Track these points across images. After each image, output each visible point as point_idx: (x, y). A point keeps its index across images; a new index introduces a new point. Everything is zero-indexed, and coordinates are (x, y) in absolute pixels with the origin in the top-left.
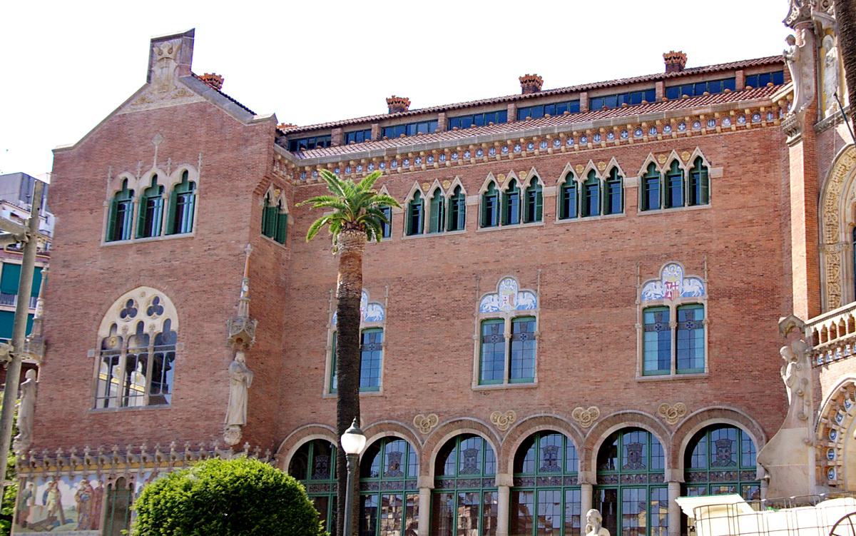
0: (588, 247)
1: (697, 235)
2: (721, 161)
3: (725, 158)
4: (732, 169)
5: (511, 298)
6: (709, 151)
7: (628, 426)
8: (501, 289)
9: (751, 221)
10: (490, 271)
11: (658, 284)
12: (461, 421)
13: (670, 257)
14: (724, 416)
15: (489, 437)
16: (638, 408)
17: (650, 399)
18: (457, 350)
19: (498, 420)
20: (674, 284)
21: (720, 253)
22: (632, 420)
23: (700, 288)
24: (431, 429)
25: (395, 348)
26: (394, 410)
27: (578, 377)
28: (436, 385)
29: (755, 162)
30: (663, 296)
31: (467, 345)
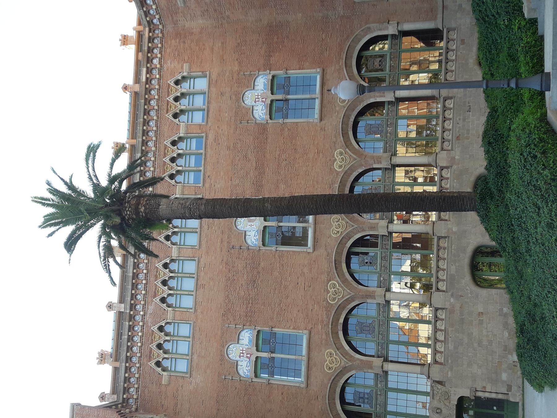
2: (180, 65)
3: (178, 63)
4: (186, 58)
6: (172, 74)
7: (351, 129)
8: (242, 229)
10: (228, 238)
11: (255, 108)
13: (239, 97)
15: (350, 238)
16: (339, 120)
17: (334, 112)
18: (283, 265)
19: (338, 230)
20: (257, 97)
22: (347, 125)
23: (262, 77)
24: (339, 288)
25: (275, 319)
27: (312, 167)
30: (264, 104)
31: (279, 256)
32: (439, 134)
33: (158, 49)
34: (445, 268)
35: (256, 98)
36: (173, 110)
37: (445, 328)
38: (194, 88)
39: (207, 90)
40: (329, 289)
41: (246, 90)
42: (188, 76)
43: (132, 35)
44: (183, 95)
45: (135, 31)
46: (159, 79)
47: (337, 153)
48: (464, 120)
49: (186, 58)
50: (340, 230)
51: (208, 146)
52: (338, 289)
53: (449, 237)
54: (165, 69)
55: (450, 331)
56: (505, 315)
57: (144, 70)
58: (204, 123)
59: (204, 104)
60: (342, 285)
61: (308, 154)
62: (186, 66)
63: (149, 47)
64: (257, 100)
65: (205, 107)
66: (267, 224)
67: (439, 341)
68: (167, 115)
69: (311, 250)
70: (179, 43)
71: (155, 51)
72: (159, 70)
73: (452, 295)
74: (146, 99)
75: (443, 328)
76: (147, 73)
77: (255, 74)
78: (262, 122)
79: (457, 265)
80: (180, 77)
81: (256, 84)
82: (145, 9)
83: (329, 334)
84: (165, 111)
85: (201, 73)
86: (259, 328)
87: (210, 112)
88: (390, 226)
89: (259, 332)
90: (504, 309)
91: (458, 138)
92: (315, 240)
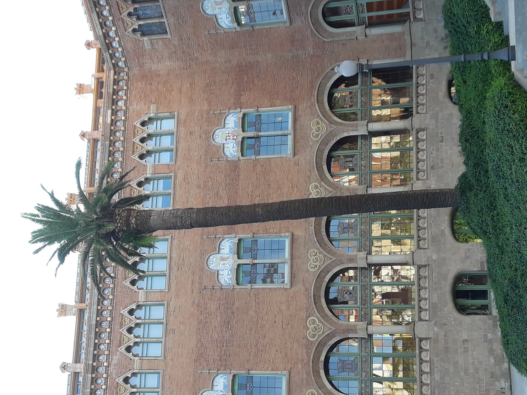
0: (192, 200)
1: (195, 120)
2: (147, 106)
3: (145, 104)
4: (153, 100)
5: (223, 259)
6: (139, 116)
7: (325, 163)
8: (215, 268)
9: (191, 84)
10: (199, 278)
11: (226, 146)
12: (314, 295)
13: (209, 136)
14: (323, 94)
16: (313, 154)
19: (316, 264)
20: (227, 135)
21: (209, 103)
25: (252, 361)
26: (302, 360)
28: (285, 321)
29: (151, 84)
30: (235, 141)
31: (255, 295)
32: (414, 166)
33: (124, 92)
34: (427, 297)
35: (227, 136)
36: (139, 151)
37: (430, 359)
38: (161, 129)
39: (175, 130)
40: (308, 325)
41: (217, 128)
42: (155, 117)
43: (89, 83)
44: (150, 136)
45: (93, 79)
46: (125, 121)
47: (312, 187)
48: (438, 150)
49: (153, 100)
50: (318, 264)
51: (177, 186)
52: (318, 325)
53: (429, 265)
54: (131, 111)
55: (435, 361)
56: (490, 342)
57: (110, 112)
58: (172, 163)
59: (172, 144)
60: (323, 320)
61: (282, 189)
62: (153, 107)
63: (114, 89)
64: (228, 138)
65: (174, 147)
66: (241, 262)
67: (425, 373)
68: (133, 157)
69: (288, 286)
70: (146, 85)
71: (120, 93)
72: (124, 112)
73: (435, 324)
74: (111, 141)
75: (428, 359)
76: (112, 115)
77: (226, 113)
78: (234, 159)
79: (439, 292)
80: (147, 118)
81: (226, 122)
82: (110, 52)
83: (310, 373)
84: (131, 152)
85: (169, 114)
86: (235, 372)
87: (179, 152)
88: (369, 257)
89: (234, 376)
90: (488, 335)
91: (433, 168)
92: (293, 276)
